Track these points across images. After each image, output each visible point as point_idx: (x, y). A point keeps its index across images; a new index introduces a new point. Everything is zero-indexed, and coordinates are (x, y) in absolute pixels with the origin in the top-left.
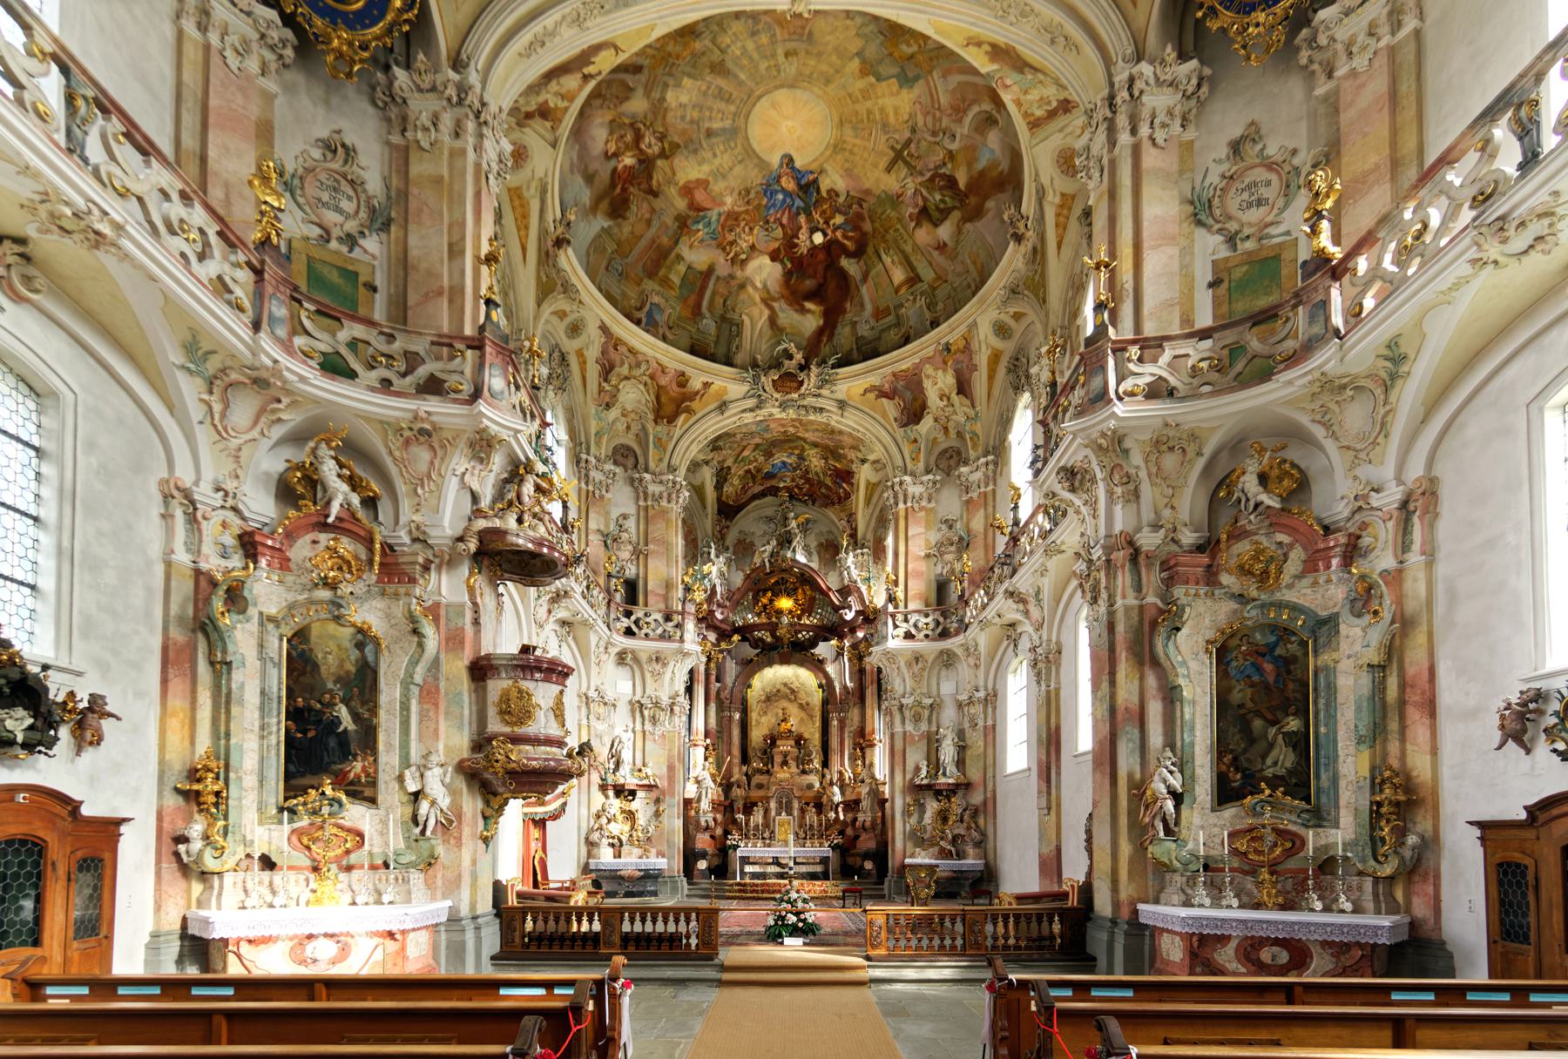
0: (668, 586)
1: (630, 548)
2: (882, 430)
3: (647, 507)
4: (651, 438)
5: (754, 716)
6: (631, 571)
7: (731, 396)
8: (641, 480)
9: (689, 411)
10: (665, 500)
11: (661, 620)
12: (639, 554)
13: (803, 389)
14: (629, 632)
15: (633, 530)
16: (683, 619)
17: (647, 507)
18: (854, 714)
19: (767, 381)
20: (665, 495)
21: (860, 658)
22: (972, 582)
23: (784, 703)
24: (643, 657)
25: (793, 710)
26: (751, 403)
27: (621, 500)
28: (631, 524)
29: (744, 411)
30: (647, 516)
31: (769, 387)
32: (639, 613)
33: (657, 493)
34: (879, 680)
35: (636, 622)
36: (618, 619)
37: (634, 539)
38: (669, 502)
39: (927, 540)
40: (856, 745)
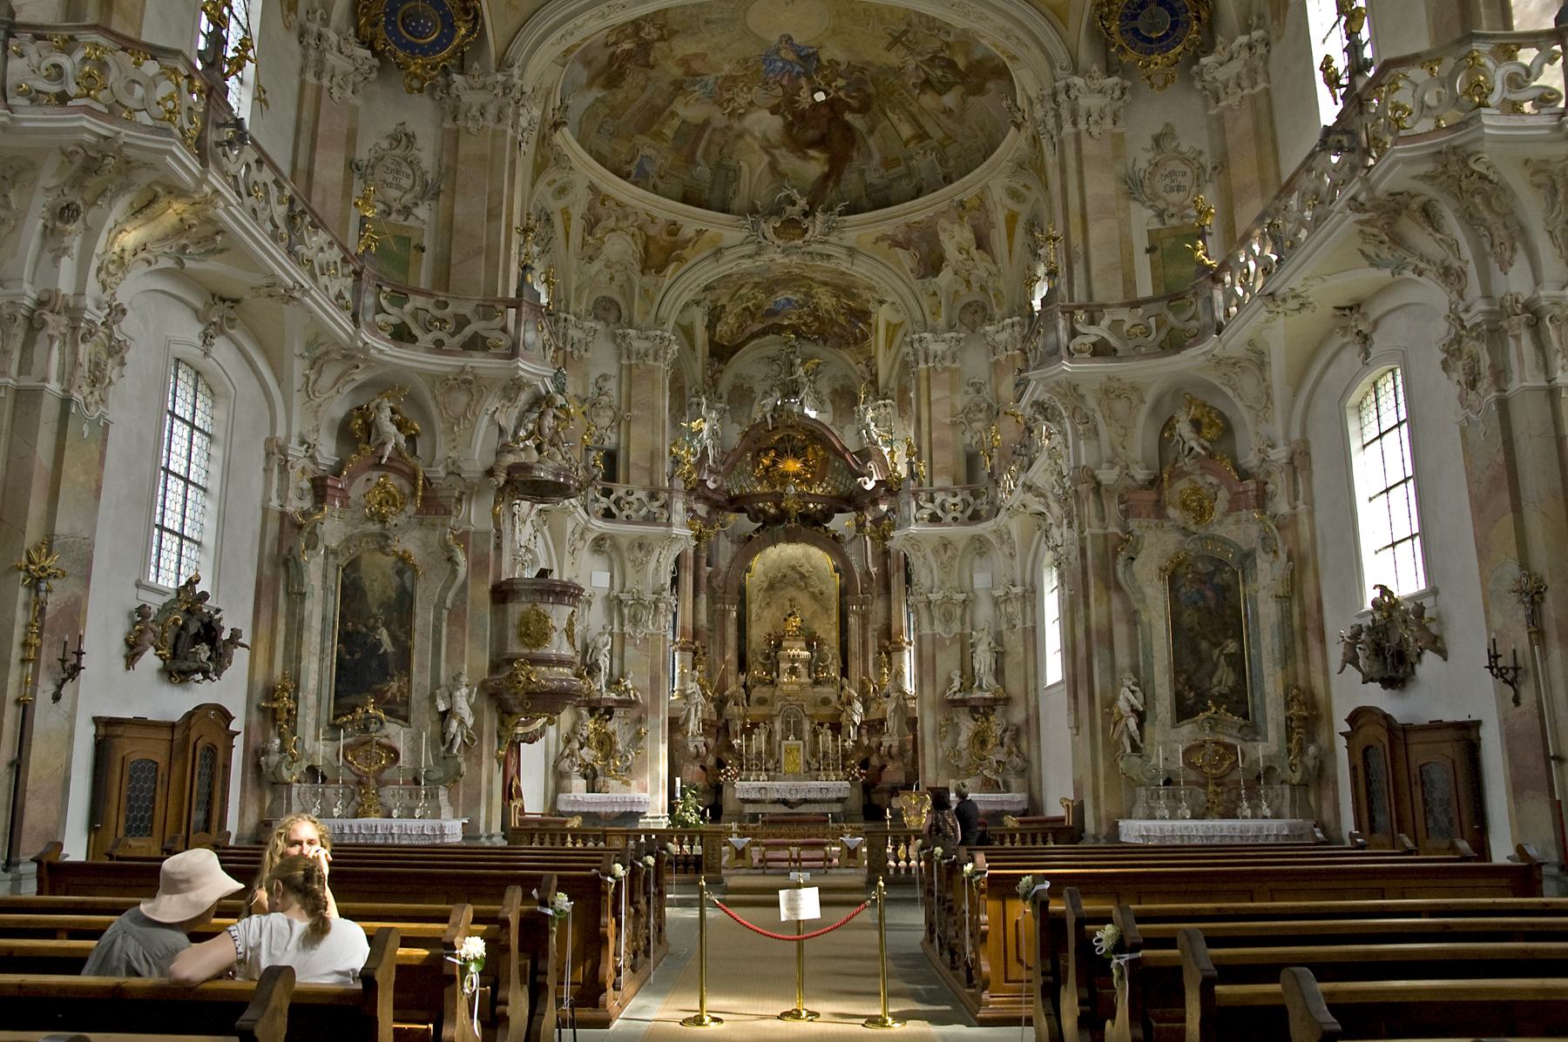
0: (654, 456)
1: (610, 413)
2: (900, 283)
3: (631, 365)
4: (637, 289)
5: (754, 608)
6: (610, 441)
7: (726, 242)
8: (624, 336)
9: (680, 259)
10: (651, 357)
11: (645, 500)
12: (621, 421)
13: (807, 237)
14: (608, 515)
15: (614, 393)
16: (671, 498)
17: (631, 365)
18: (878, 607)
19: (768, 227)
20: (651, 352)
21: (885, 538)
22: (1002, 456)
23: (792, 592)
24: (624, 543)
25: (803, 598)
26: (750, 249)
27: (602, 359)
28: (611, 386)
29: (743, 257)
30: (629, 375)
31: (770, 234)
32: (620, 490)
33: (642, 351)
34: (907, 564)
35: (617, 502)
36: (597, 500)
37: (615, 403)
38: (656, 360)
39: (953, 405)
40: (882, 648)
